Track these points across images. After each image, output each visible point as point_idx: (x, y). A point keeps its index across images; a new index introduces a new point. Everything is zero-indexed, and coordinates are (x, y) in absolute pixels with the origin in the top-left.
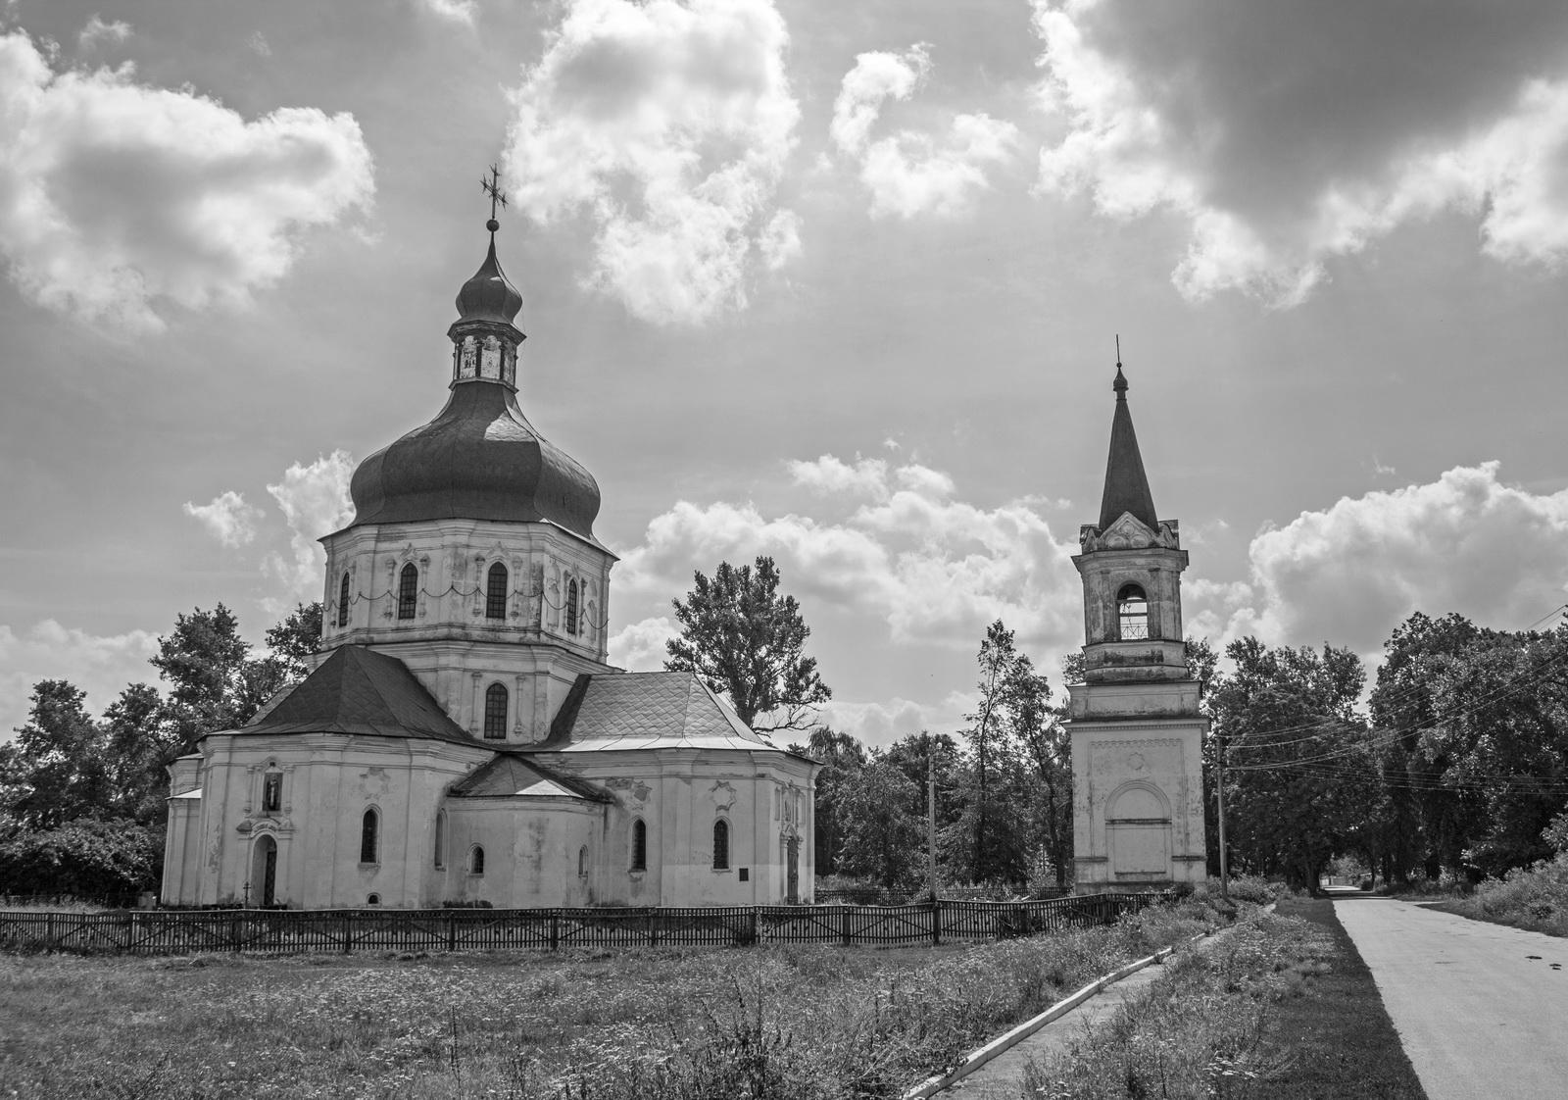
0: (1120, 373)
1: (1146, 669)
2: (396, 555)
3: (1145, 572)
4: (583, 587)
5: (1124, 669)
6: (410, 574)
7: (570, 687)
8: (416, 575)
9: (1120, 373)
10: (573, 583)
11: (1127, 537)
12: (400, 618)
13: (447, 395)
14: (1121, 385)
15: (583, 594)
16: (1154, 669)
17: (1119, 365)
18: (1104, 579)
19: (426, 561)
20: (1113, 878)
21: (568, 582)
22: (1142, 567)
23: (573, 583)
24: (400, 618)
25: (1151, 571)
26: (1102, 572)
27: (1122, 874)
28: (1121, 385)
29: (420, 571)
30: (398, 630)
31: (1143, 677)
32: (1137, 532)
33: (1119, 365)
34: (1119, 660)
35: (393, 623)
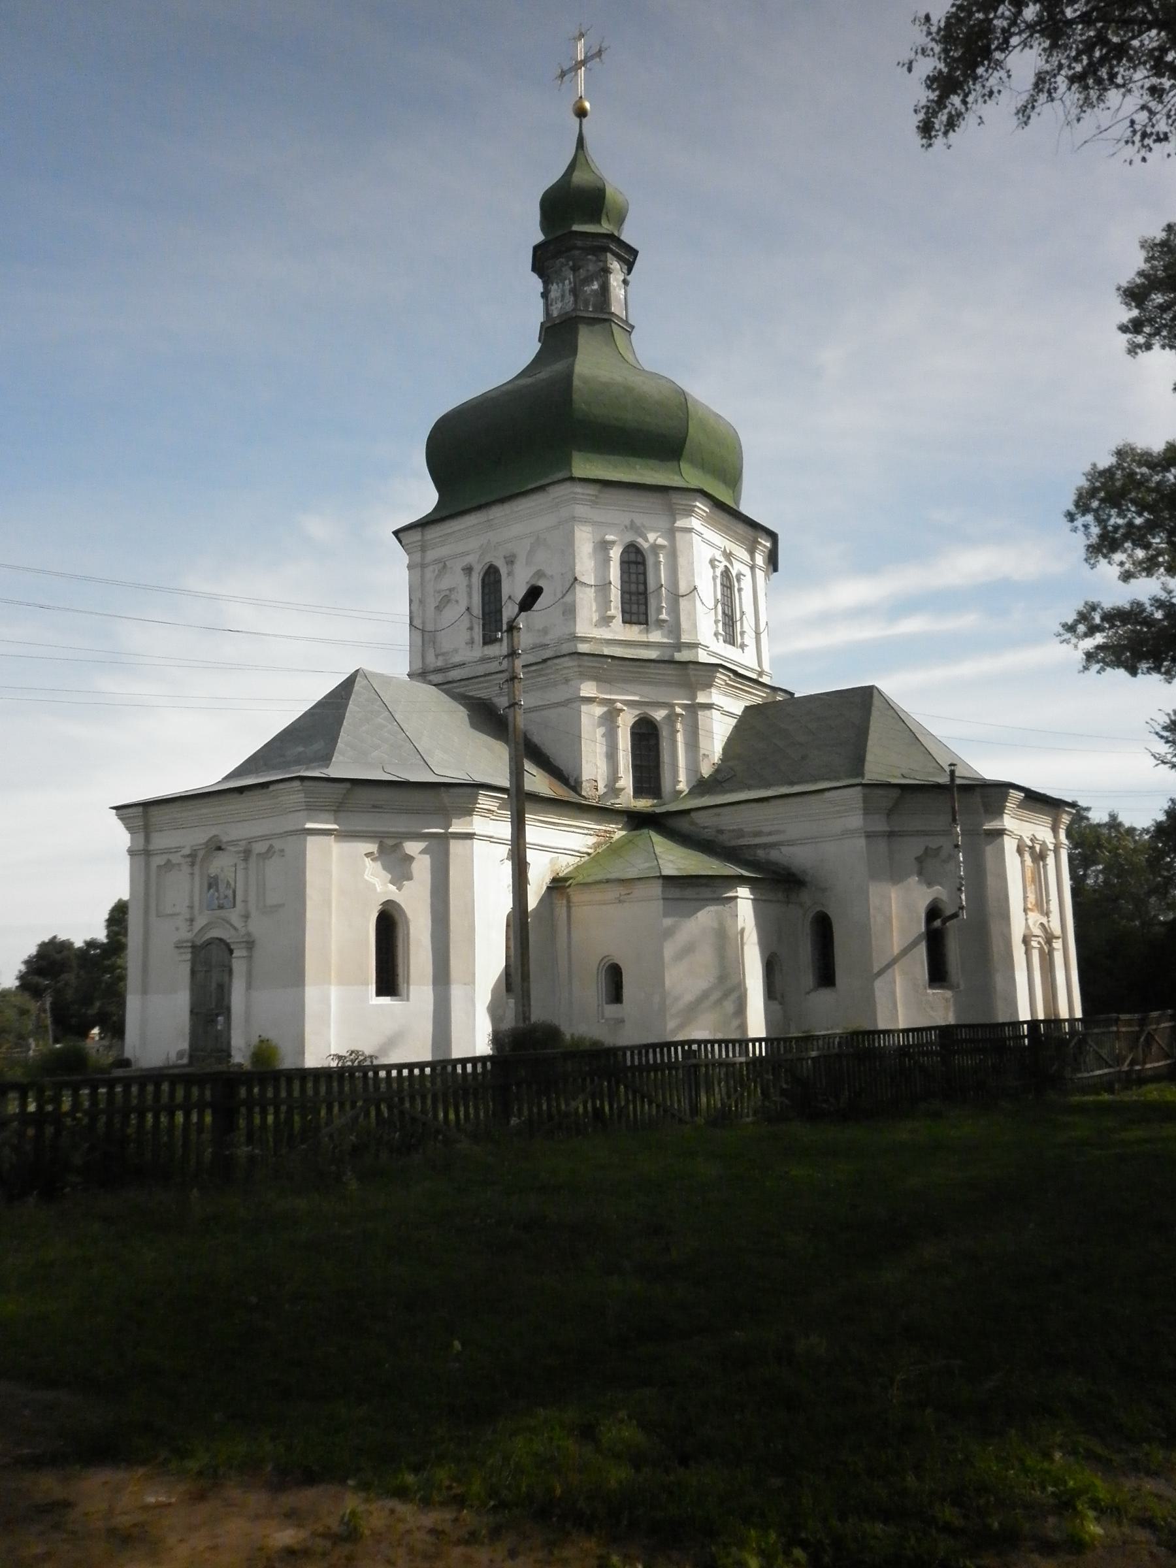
2: (470, 559)
4: (739, 580)
6: (491, 580)
7: (734, 722)
8: (499, 581)
10: (726, 573)
12: (485, 643)
13: (533, 347)
15: (740, 590)
19: (510, 561)
21: (718, 572)
23: (726, 573)
24: (485, 643)
29: (503, 571)
30: (484, 660)
35: (478, 651)
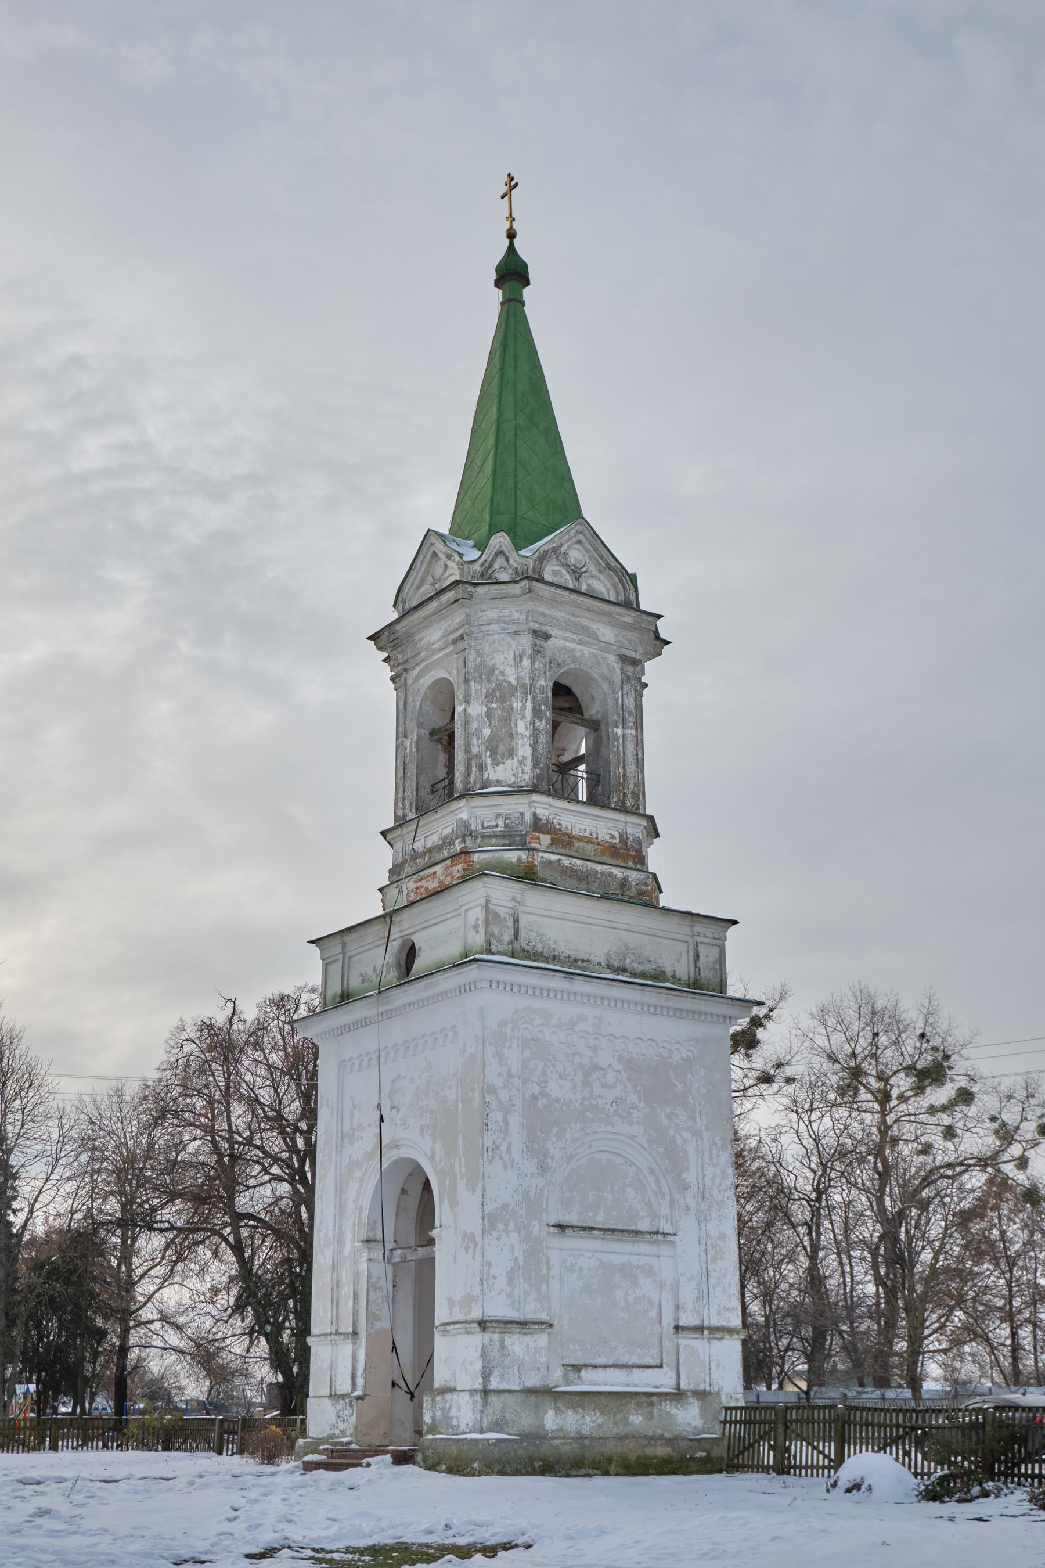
0: (511, 249)
1: (616, 871)
3: (612, 658)
5: (566, 861)
9: (511, 249)
11: (577, 573)
14: (512, 274)
16: (634, 876)
17: (511, 235)
18: (537, 652)
20: (556, 1378)
22: (606, 647)
25: (624, 659)
26: (535, 632)
27: (577, 1368)
28: (512, 274)
31: (614, 888)
32: (592, 568)
33: (511, 235)
34: (562, 840)
